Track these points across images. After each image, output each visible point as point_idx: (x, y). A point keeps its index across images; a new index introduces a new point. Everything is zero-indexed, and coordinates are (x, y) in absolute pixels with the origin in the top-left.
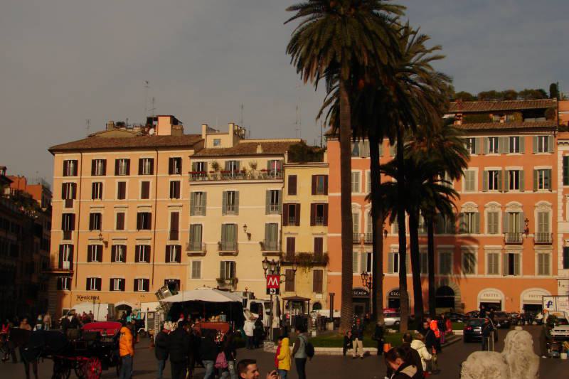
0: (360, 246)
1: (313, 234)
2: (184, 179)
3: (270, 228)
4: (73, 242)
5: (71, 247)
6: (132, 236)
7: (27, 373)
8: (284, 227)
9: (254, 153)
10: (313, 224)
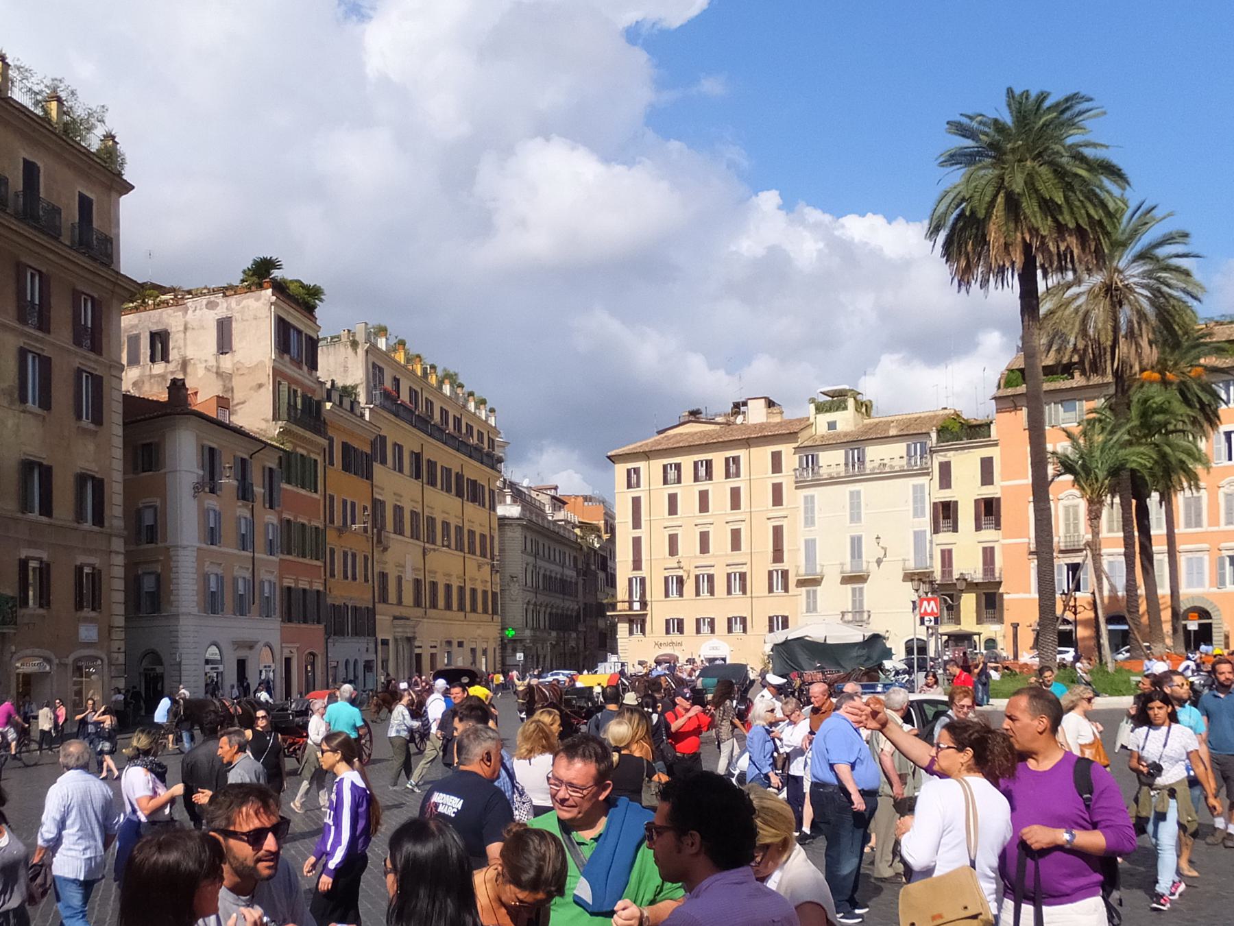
2: (786, 479)
3: (918, 536)
4: (644, 573)
5: (643, 581)
6: (720, 560)
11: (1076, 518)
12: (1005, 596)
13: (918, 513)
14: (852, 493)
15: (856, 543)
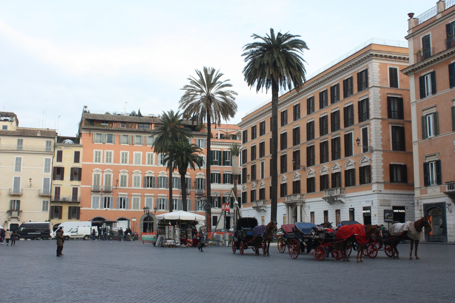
0: (100, 193)
1: (72, 185)
3: (46, 180)
7: (412, 249)
8: (53, 181)
9: (36, 135)
10: (72, 179)
11: (110, 180)
12: (81, 208)
13: (47, 170)
14: (17, 158)
15: (17, 180)
